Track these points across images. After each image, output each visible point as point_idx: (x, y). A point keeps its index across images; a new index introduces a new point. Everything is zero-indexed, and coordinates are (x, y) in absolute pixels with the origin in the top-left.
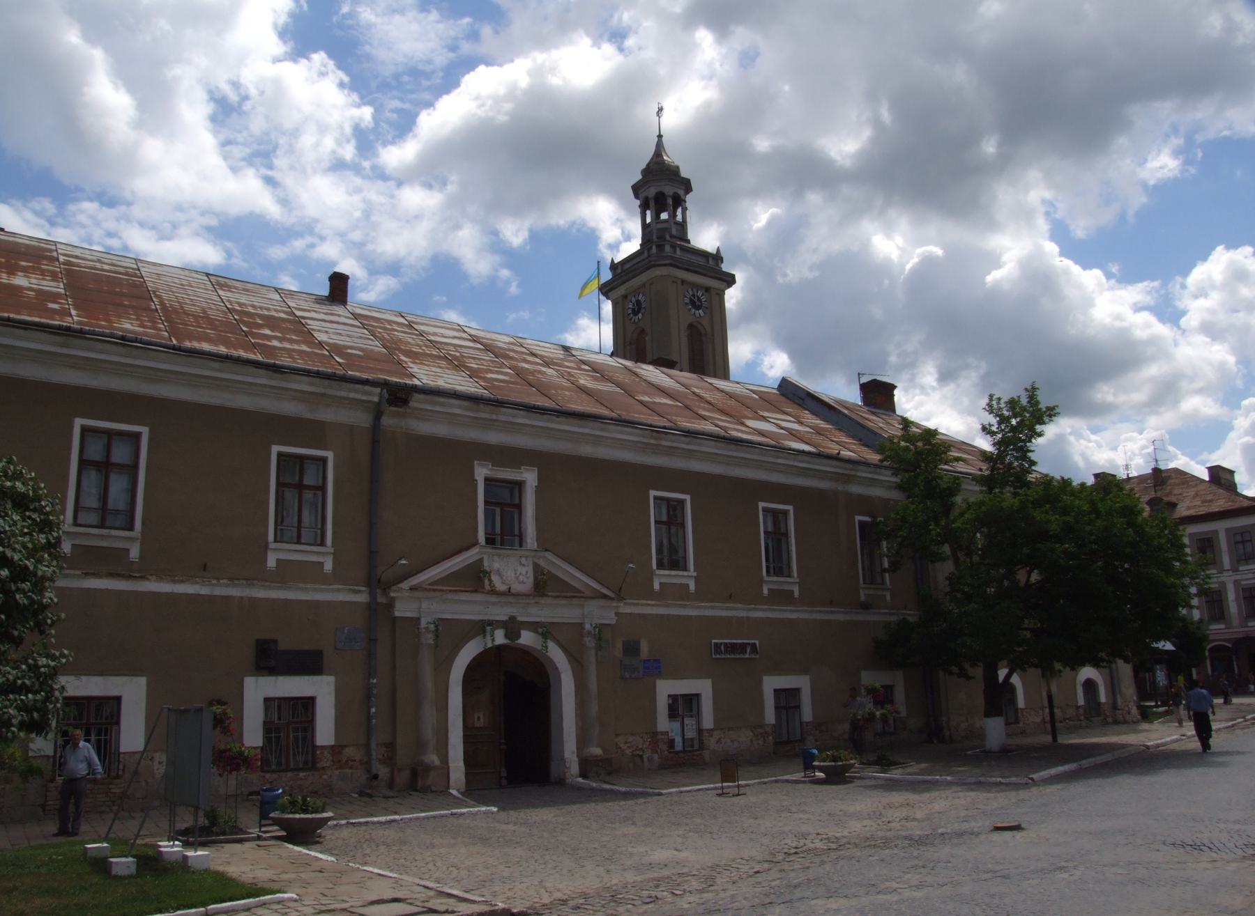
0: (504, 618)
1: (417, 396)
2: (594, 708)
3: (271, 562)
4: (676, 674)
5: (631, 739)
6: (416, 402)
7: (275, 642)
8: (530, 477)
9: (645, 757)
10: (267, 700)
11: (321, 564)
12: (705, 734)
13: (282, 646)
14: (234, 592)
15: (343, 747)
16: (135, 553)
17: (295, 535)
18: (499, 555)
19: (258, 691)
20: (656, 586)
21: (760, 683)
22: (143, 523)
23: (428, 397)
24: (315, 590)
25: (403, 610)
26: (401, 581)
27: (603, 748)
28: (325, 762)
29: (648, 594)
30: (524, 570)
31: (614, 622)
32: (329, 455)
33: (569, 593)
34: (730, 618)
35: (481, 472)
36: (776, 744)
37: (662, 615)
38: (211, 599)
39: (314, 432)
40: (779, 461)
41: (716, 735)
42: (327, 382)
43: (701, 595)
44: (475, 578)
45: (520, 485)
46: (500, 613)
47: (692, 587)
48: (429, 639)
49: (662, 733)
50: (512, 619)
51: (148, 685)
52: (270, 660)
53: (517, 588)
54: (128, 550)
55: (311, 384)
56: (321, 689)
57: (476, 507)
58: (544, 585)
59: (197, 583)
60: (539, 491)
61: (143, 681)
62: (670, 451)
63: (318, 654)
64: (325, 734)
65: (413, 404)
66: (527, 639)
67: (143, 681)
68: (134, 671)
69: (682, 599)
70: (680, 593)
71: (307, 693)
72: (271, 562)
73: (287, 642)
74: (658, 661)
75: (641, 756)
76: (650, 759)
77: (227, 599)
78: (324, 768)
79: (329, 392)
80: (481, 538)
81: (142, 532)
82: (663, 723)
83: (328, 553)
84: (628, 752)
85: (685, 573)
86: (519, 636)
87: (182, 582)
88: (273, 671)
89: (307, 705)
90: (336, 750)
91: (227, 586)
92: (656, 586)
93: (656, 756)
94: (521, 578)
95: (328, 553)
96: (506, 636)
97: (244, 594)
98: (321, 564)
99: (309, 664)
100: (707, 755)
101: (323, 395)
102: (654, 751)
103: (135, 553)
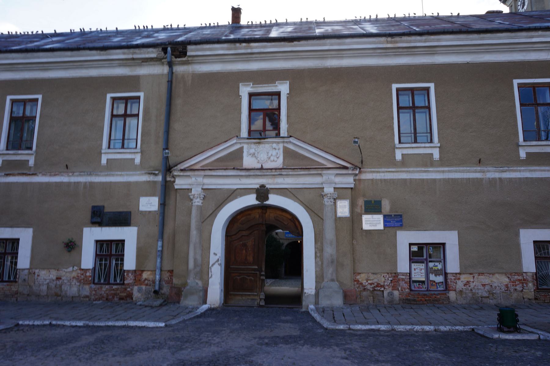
0: (257, 186)
1: (189, 47)
2: (329, 251)
3: (104, 161)
4: (417, 225)
5: (372, 277)
6: (192, 51)
8: (284, 88)
10: (97, 242)
11: (133, 160)
12: (449, 277)
13: (106, 210)
14: (82, 179)
16: (32, 163)
17: (121, 144)
19: (92, 236)
20: (399, 157)
21: (517, 235)
22: (37, 146)
23: (199, 47)
24: (127, 175)
25: (180, 183)
26: (176, 165)
28: (129, 280)
29: (391, 162)
30: (274, 152)
31: (352, 186)
32: (141, 94)
33: (316, 168)
34: (479, 181)
35: (245, 90)
36: (538, 290)
37: (405, 180)
38: (69, 184)
39: (133, 82)
40: (534, 40)
41: (464, 278)
42: (132, 50)
43: (444, 161)
44: (233, 162)
45: (278, 94)
46: (255, 183)
47: (436, 155)
48: (198, 202)
49: (403, 274)
50: (263, 186)
51: (34, 232)
52: (99, 217)
54: (28, 161)
55: (124, 54)
56: (129, 235)
57: (240, 113)
58: (295, 163)
59: (62, 175)
60: (290, 96)
61: (30, 231)
62: (410, 51)
63: (129, 214)
64: (130, 262)
65: (188, 54)
66: (274, 200)
67: (30, 231)
68: (27, 225)
69: (426, 166)
70: (426, 161)
71: (16, 236)
72: (104, 161)
73: (111, 207)
75: (383, 291)
76: (390, 294)
77: (77, 184)
78: (128, 284)
79: (135, 56)
80: (244, 133)
81: (36, 151)
82: (403, 265)
83: (137, 153)
85: (431, 145)
86: (267, 199)
87: (55, 175)
88: (100, 224)
90: (138, 273)
91: (77, 176)
92: (399, 157)
93: (396, 293)
94: (272, 158)
95: (137, 153)
96: (257, 199)
97: (87, 181)
98: (133, 160)
99: (122, 219)
100: (452, 295)
101: (133, 59)
102: (395, 288)
103: (32, 163)
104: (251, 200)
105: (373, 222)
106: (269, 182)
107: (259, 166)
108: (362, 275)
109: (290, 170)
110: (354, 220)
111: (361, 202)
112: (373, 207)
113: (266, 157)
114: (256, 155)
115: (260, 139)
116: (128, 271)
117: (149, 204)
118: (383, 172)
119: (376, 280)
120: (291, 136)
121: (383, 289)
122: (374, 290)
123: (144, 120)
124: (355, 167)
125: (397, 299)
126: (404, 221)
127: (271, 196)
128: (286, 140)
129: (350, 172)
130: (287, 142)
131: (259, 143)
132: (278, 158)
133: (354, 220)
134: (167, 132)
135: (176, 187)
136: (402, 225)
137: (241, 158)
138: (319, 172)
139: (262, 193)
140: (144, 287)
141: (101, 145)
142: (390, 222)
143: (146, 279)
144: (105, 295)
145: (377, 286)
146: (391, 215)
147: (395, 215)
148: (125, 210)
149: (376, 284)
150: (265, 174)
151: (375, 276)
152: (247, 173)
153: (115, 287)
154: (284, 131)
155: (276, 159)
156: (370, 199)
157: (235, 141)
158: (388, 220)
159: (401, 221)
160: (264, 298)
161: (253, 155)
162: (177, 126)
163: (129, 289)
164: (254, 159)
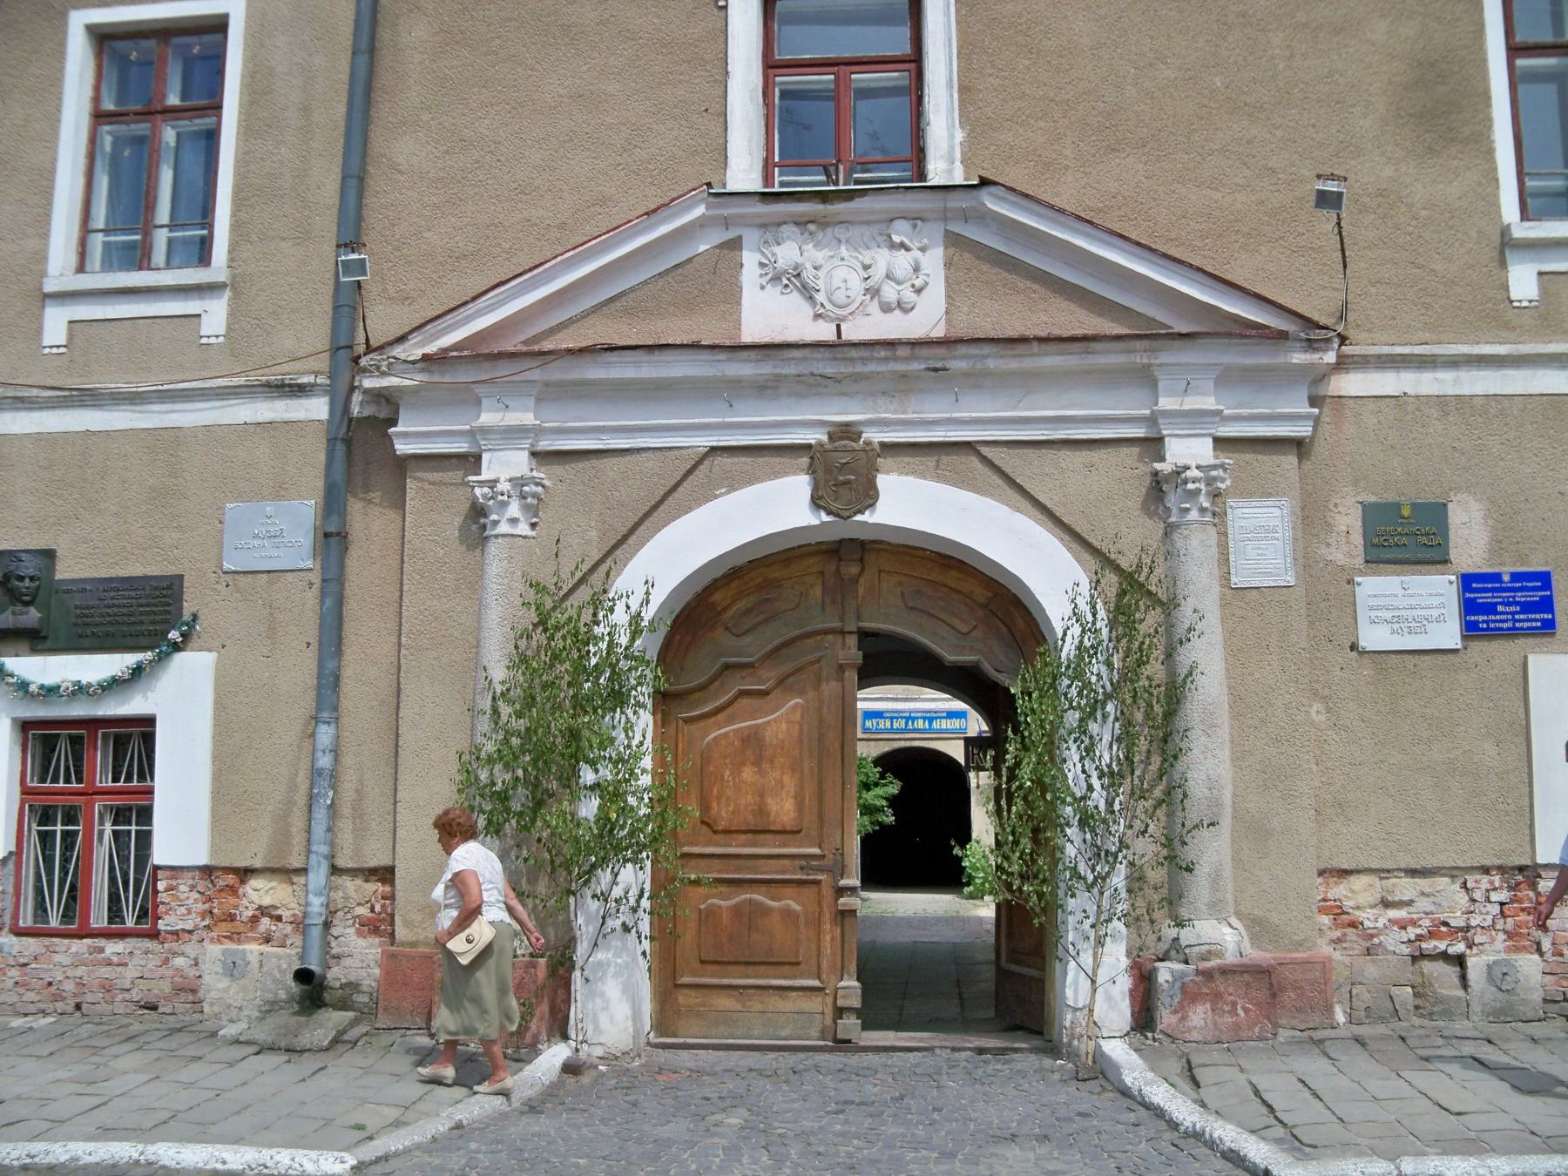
5: (1405, 888)
7: (49, 555)
9: (1476, 965)
15: (245, 873)
18: (801, 223)
26: (402, 339)
27: (1258, 928)
28: (181, 909)
31: (1303, 430)
46: (805, 421)
50: (846, 432)
53: (870, 326)
64: (181, 831)
66: (907, 504)
74: (1545, 579)
75: (1460, 961)
76: (1499, 976)
78: (176, 934)
84: (1395, 941)
86: (868, 496)
89: (134, 741)
93: (1529, 966)
94: (890, 293)
96: (817, 502)
99: (145, 617)
104: (782, 507)
105: (1413, 610)
106: (879, 420)
107: (825, 332)
108: (1359, 882)
109: (987, 349)
110: (1324, 598)
111: (1348, 520)
112: (1405, 537)
113: (856, 286)
114: (809, 273)
115: (823, 197)
116: (175, 870)
117: (275, 532)
118: (1454, 362)
119: (1424, 904)
120: (984, 182)
121: (1460, 947)
122: (1418, 957)
123: (248, 128)
124: (1313, 332)
125: (1537, 996)
126: (1560, 604)
127: (886, 482)
128: (957, 202)
129: (1299, 358)
130: (965, 216)
131: (823, 223)
132: (919, 291)
133: (1324, 598)
134: (355, 179)
135: (402, 448)
136: (1549, 625)
137: (732, 296)
138: (1140, 359)
139: (843, 472)
140: (253, 949)
141: (41, 258)
142: (1490, 609)
143: (263, 911)
144: (69, 986)
145: (1432, 935)
146: (1496, 577)
147: (1516, 577)
148: (154, 570)
149: (1426, 923)
150: (859, 368)
151: (1423, 883)
152: (766, 369)
153: (113, 948)
154: (944, 166)
155: (909, 296)
156: (1391, 497)
157: (700, 210)
158: (1484, 598)
159: (1547, 605)
160: (856, 1002)
161: (796, 281)
162: (403, 150)
163: (179, 962)
164: (796, 298)
